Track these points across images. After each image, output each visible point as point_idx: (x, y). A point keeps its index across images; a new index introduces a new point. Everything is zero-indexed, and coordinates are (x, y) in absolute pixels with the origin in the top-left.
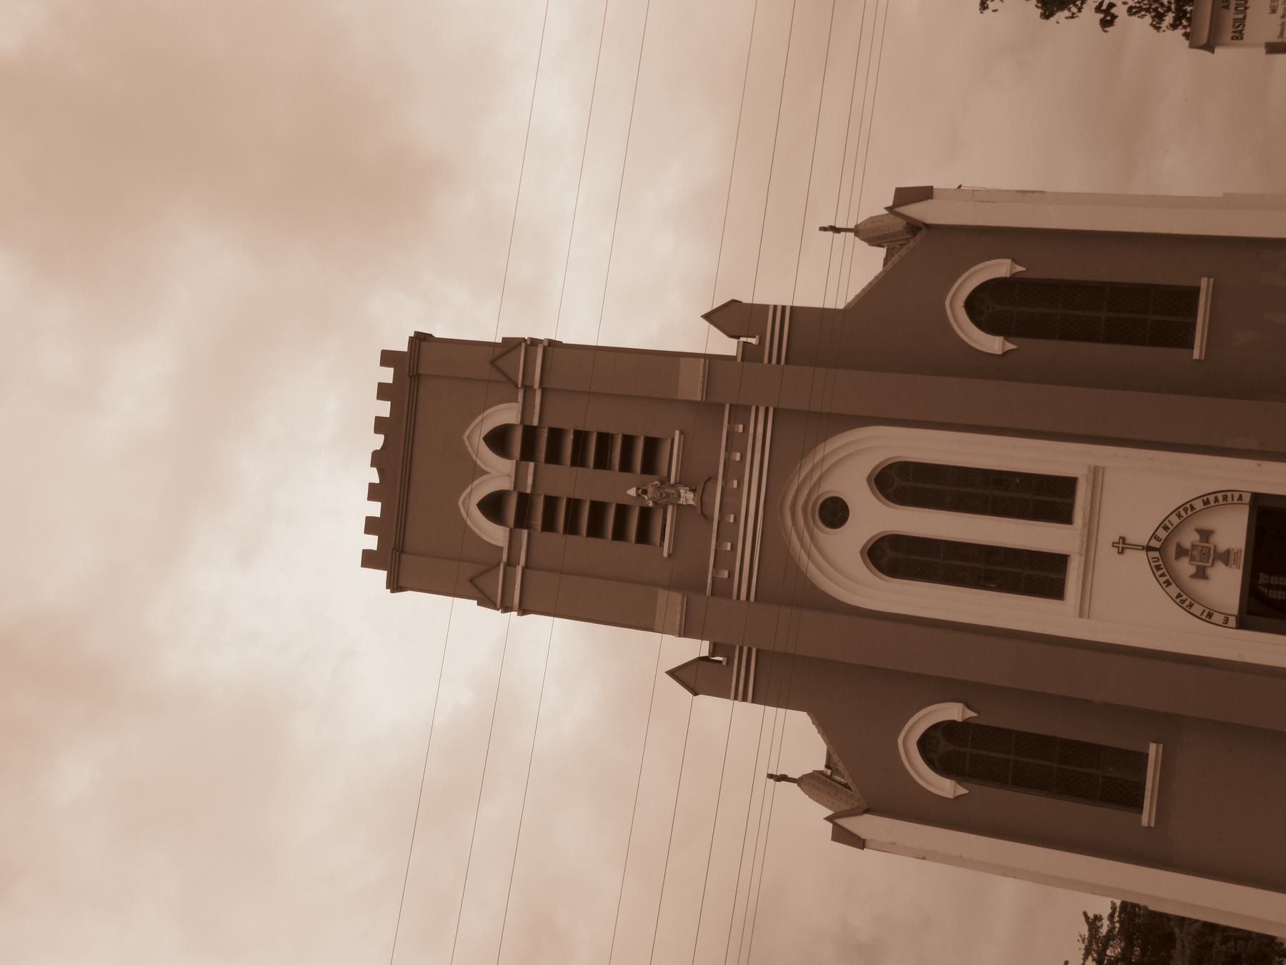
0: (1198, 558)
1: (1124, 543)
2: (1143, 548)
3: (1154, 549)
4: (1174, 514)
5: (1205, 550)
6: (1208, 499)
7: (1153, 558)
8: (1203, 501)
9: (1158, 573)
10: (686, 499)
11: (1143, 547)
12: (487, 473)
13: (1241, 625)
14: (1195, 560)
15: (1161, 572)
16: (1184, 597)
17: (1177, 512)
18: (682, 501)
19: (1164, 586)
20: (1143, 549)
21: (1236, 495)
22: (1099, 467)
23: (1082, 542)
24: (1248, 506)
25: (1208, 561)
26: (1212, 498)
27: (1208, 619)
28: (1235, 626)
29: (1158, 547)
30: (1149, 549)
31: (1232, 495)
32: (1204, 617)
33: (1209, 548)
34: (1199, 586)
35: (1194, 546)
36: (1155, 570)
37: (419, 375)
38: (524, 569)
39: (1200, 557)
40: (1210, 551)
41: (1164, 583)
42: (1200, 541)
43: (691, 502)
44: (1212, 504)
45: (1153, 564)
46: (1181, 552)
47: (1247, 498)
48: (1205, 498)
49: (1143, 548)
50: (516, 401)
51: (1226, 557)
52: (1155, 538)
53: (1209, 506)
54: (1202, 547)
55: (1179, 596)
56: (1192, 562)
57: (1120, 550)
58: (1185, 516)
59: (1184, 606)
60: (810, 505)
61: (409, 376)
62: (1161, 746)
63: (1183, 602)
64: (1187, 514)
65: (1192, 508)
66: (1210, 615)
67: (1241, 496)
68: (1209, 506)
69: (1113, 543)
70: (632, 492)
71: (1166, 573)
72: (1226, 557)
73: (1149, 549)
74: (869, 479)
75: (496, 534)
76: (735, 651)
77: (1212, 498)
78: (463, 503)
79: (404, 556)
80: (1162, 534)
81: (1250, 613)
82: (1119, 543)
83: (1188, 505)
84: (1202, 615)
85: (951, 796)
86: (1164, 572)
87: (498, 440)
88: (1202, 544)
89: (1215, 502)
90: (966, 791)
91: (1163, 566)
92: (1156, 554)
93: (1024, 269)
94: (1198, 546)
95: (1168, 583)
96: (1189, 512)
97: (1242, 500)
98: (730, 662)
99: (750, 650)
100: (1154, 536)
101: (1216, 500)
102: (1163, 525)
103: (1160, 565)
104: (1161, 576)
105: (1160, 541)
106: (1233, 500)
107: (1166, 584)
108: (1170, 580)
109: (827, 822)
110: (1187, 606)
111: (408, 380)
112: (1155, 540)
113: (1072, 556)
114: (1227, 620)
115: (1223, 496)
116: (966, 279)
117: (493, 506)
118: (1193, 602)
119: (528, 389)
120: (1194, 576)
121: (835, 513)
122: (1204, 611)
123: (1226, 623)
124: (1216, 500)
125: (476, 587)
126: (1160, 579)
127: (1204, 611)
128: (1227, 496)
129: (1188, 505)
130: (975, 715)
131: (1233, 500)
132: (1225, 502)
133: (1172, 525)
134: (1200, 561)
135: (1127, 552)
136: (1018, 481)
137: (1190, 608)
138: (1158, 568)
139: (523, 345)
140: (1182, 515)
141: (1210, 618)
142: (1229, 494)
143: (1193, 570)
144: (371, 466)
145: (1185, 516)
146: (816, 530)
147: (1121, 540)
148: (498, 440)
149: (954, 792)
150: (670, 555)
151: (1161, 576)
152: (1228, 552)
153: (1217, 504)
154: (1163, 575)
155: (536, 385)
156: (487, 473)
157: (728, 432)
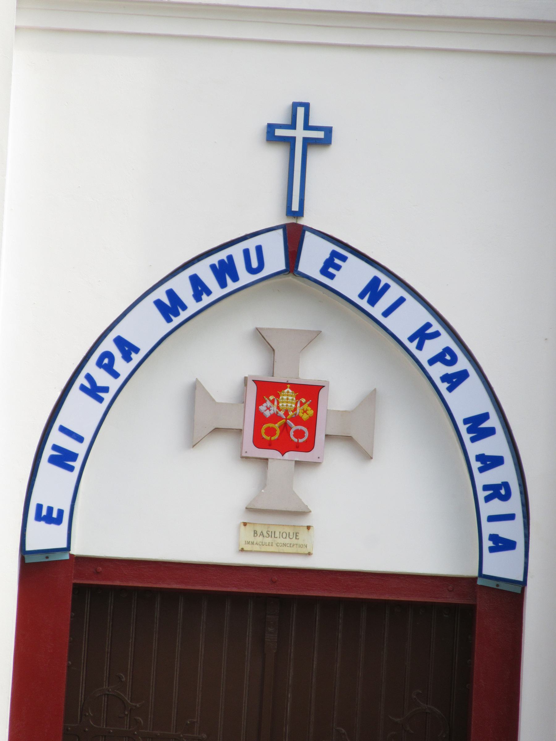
0: (268, 408)
4: (429, 318)
5: (299, 434)
6: (491, 431)
7: (259, 249)
8: (485, 417)
11: (300, 213)
14: (260, 401)
15: (210, 280)
17: (436, 326)
19: (161, 294)
20: (290, 212)
25: (259, 442)
28: (28, 548)
29: (302, 268)
31: (511, 517)
36: (214, 259)
39: (275, 418)
40: (298, 448)
45: (236, 252)
48: (493, 422)
52: (334, 254)
53: (466, 437)
54: (312, 424)
56: (253, 390)
57: (279, 132)
59: (91, 368)
64: (432, 362)
67: (509, 545)
68: (466, 437)
69: (306, 106)
81: (79, 590)
82: (307, 127)
84: (62, 429)
89: (480, 458)
94: (315, 406)
97: (492, 550)
102: (384, 279)
103: (235, 278)
104: (195, 281)
105: (324, 271)
106: (491, 519)
107: (166, 301)
108: (184, 315)
110: (89, 377)
112: (327, 256)
115: (506, 485)
118: (107, 397)
122: (80, 439)
123: (39, 517)
127: (80, 439)
128: (506, 497)
129: (463, 364)
131: (491, 519)
132: (482, 494)
133: (386, 314)
134: (259, 416)
137: (83, 388)
140: (428, 343)
141: (53, 460)
145: (424, 356)
147: (320, 135)
151: (195, 281)
152: (303, 513)
153: (476, 465)
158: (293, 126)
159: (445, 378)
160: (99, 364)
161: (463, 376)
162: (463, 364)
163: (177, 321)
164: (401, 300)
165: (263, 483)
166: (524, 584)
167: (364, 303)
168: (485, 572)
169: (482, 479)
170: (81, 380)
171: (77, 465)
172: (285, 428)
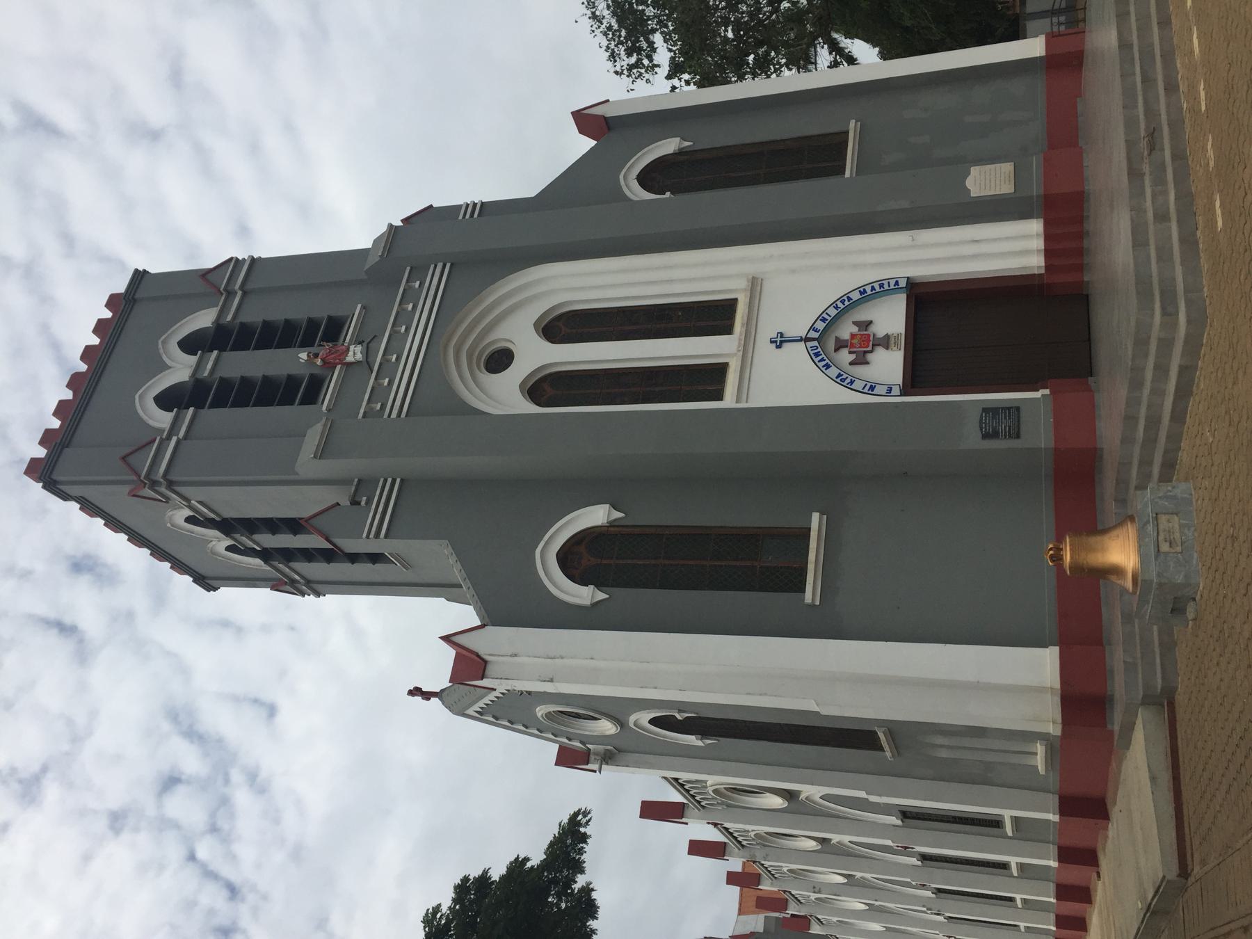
1: (781, 337)
2: (801, 340)
3: (813, 339)
9: (816, 360)
10: (354, 353)
11: (801, 337)
12: (170, 367)
13: (904, 392)
14: (855, 348)
15: (820, 357)
16: (844, 377)
17: (834, 305)
18: (350, 358)
19: (823, 369)
21: (892, 283)
22: (758, 279)
23: (740, 340)
24: (904, 296)
25: (868, 346)
26: (868, 289)
27: (870, 392)
30: (807, 340)
31: (889, 282)
32: (866, 390)
33: (869, 335)
34: (860, 371)
35: (853, 336)
36: (814, 357)
37: (135, 301)
38: (178, 442)
41: (823, 367)
42: (859, 331)
43: (359, 357)
44: (869, 292)
45: (811, 353)
46: (840, 345)
47: (903, 283)
48: (862, 289)
49: (801, 340)
50: (217, 306)
51: (886, 342)
52: (813, 330)
53: (866, 295)
54: (860, 335)
55: (839, 375)
57: (778, 344)
58: (842, 307)
59: (845, 384)
60: (475, 357)
61: (124, 299)
62: (825, 516)
63: (843, 380)
65: (849, 299)
66: (872, 388)
68: (866, 295)
70: (303, 356)
71: (825, 358)
72: (886, 342)
73: (807, 340)
74: (536, 325)
75: (162, 419)
76: (378, 486)
77: (868, 289)
78: (140, 396)
79: (66, 450)
80: (821, 326)
83: (845, 298)
85: (587, 602)
86: (821, 358)
87: (188, 345)
88: (859, 333)
89: (872, 291)
90: (606, 596)
91: (821, 352)
92: (815, 343)
93: (692, 143)
95: (827, 366)
96: (847, 303)
98: (369, 502)
99: (394, 481)
100: (813, 328)
101: (873, 288)
102: (821, 318)
104: (819, 362)
106: (889, 286)
108: (830, 363)
109: (442, 642)
110: (848, 384)
111: (124, 302)
113: (730, 364)
114: (890, 390)
116: (639, 157)
117: (166, 400)
118: (853, 379)
119: (230, 294)
120: (851, 364)
121: (500, 360)
122: (866, 384)
123: (890, 393)
124: (873, 288)
125: (129, 465)
126: (819, 364)
127: (866, 384)
128: (883, 284)
130: (621, 515)
131: (889, 286)
133: (830, 316)
134: (860, 347)
135: (785, 345)
136: (680, 314)
138: (817, 355)
139: (233, 261)
141: (872, 391)
142: (886, 283)
143: (853, 357)
144: (67, 386)
146: (477, 372)
148: (188, 345)
149: (592, 597)
150: (329, 410)
151: (819, 362)
152: (887, 337)
154: (822, 360)
155: (237, 287)
156: (170, 367)
157: (404, 290)
158: (776, 342)
159: (849, 301)
160: (843, 382)
161: (848, 297)
162: (845, 298)
163: (831, 364)
164: (827, 313)
165: (879, 345)
166: (908, 278)
167: (827, 322)
168: (905, 286)
169: (878, 289)
170: (848, 386)
171: (874, 385)
172: (863, 341)
